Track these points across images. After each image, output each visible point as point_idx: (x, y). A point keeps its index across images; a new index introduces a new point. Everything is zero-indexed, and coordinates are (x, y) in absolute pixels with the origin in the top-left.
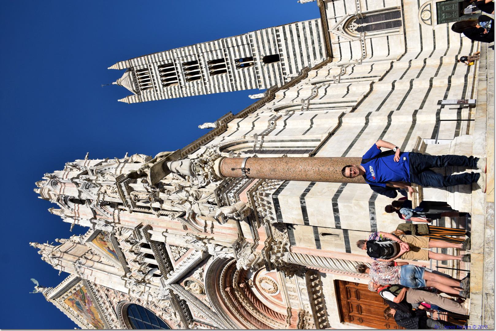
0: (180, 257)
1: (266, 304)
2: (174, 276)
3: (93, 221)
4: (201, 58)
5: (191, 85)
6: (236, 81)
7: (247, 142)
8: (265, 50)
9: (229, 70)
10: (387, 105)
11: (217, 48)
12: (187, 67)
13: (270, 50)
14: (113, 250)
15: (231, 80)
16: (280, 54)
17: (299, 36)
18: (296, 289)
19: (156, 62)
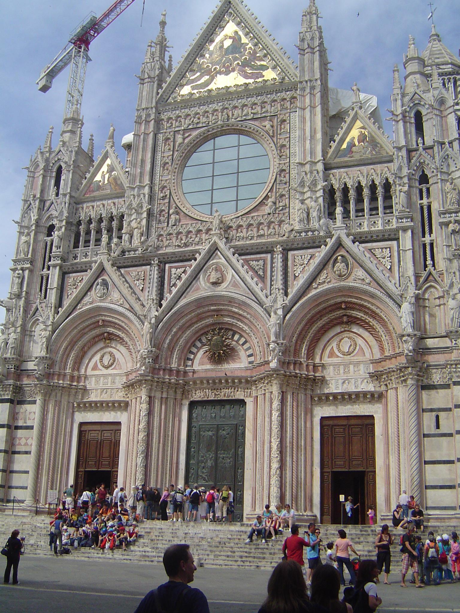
0: (377, 258)
1: (321, 339)
3: (405, 149)
14: (352, 152)
18: (348, 375)
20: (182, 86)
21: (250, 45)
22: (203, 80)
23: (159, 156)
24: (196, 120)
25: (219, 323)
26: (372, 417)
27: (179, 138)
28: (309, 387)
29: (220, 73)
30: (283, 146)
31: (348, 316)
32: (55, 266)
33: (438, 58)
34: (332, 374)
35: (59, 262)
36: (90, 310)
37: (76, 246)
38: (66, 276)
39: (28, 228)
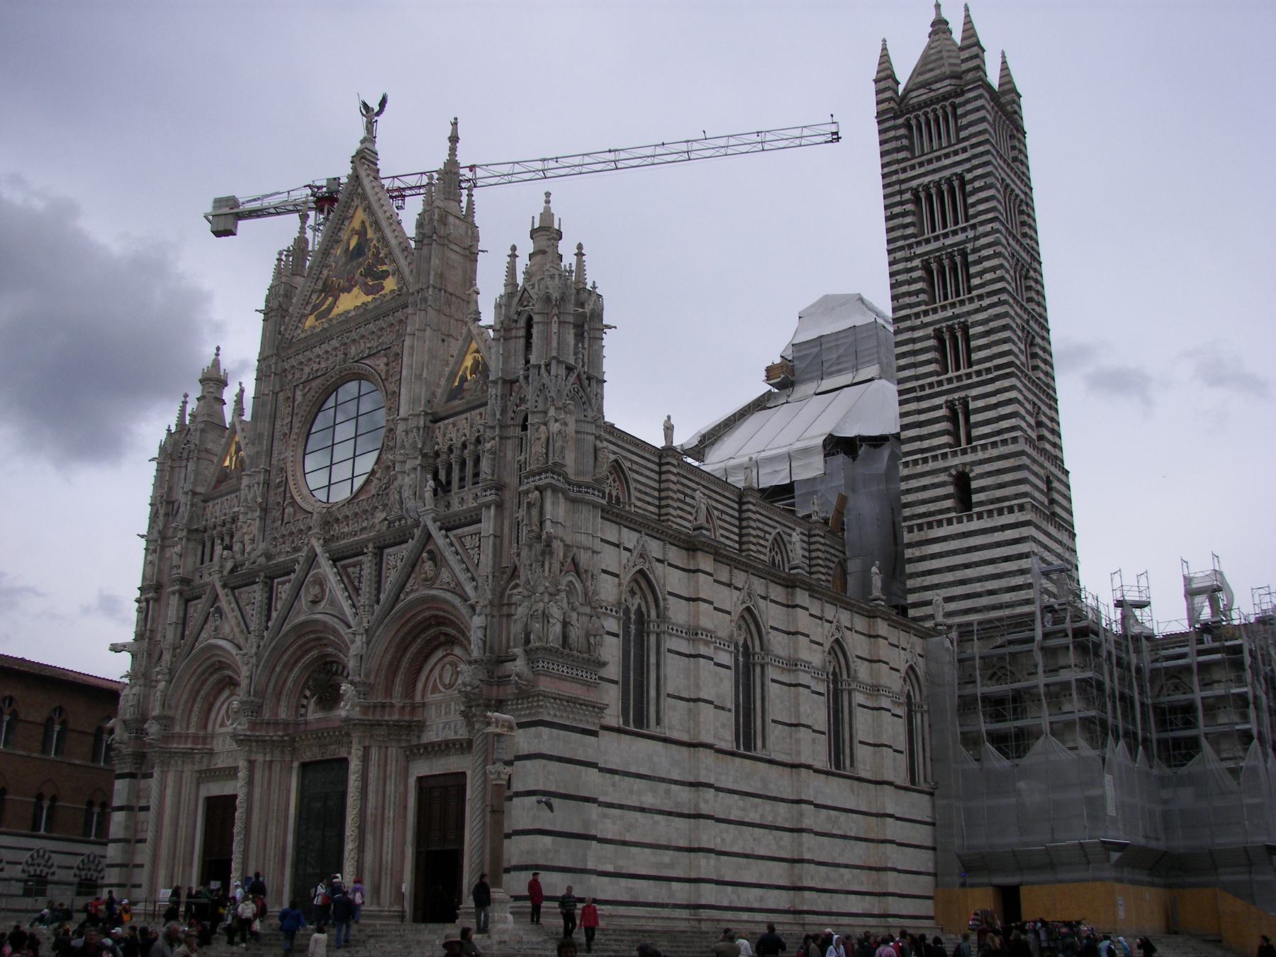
2: (439, 537)
3: (500, 382)
4: (976, 305)
5: (915, 275)
6: (919, 399)
7: (657, 606)
8: (981, 476)
9: (945, 383)
10: (741, 803)
11: (995, 350)
12: (958, 259)
13: (982, 489)
15: (922, 388)
16: (971, 515)
17: (1007, 559)
19: (969, 171)
20: (306, 316)
21: (375, 242)
22: (328, 302)
23: (278, 423)
24: (316, 367)
25: (327, 655)
26: (464, 774)
27: (299, 394)
28: (404, 738)
29: (343, 290)
30: (394, 392)
31: (445, 634)
32: (173, 593)
33: (932, 70)
34: (433, 717)
35: (177, 587)
36: (204, 649)
37: (202, 563)
38: (190, 604)
39: (156, 541)
